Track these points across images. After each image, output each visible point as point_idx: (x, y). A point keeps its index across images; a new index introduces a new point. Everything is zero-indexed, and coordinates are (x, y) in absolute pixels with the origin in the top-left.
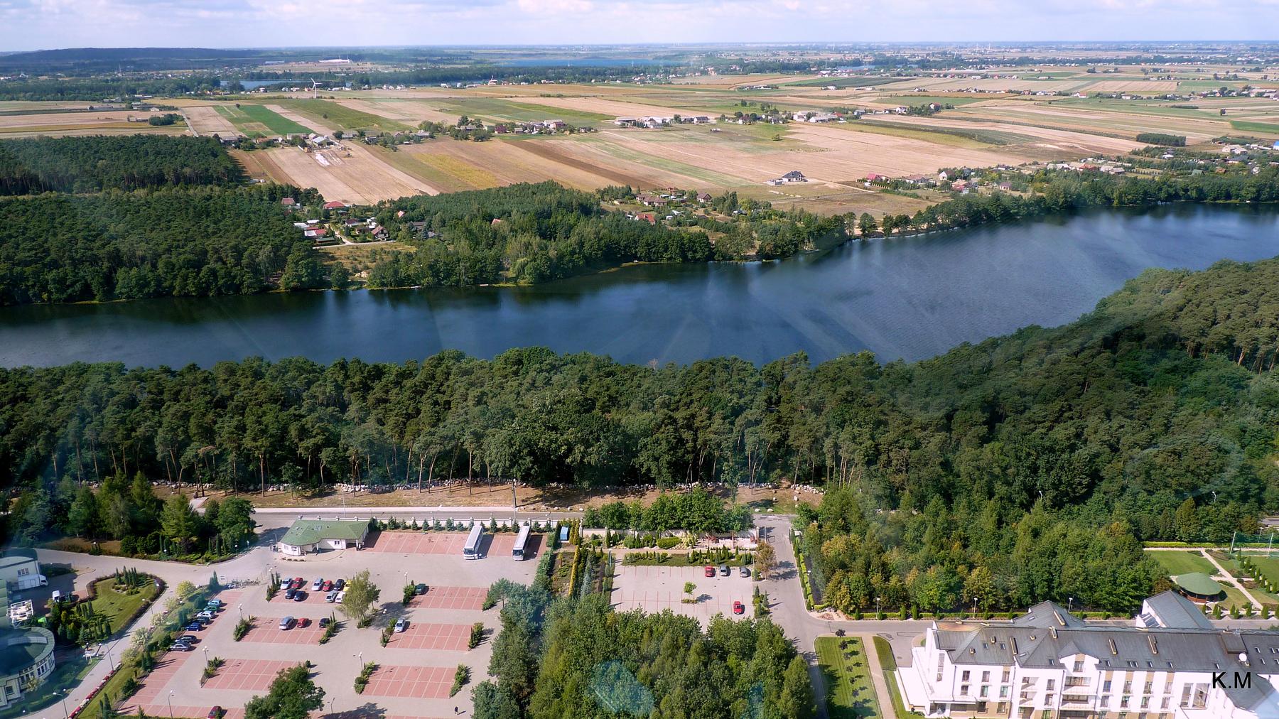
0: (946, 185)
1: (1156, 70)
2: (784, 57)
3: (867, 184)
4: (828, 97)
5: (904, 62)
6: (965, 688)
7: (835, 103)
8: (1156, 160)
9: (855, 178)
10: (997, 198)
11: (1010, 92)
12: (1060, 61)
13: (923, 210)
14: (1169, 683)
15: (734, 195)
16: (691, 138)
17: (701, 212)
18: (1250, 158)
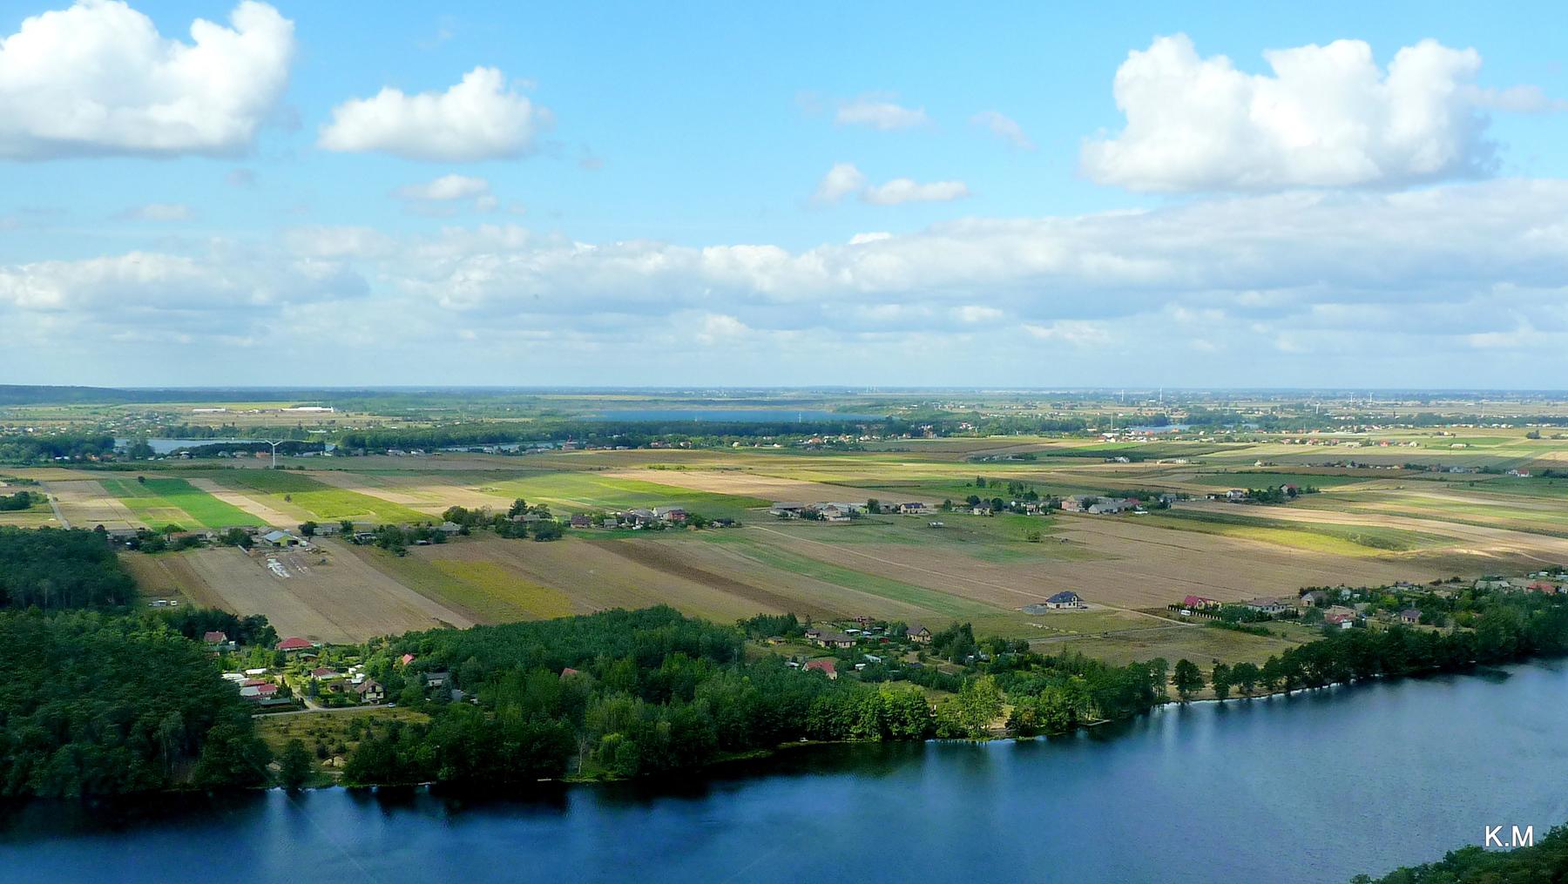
0: (1312, 616)
2: (1044, 412)
3: (1185, 613)
4: (1117, 474)
5: (1235, 420)
7: (1128, 483)
9: (1164, 603)
10: (1397, 633)
11: (1408, 466)
12: (1484, 420)
13: (1279, 656)
15: (967, 630)
16: (895, 537)
17: (912, 657)
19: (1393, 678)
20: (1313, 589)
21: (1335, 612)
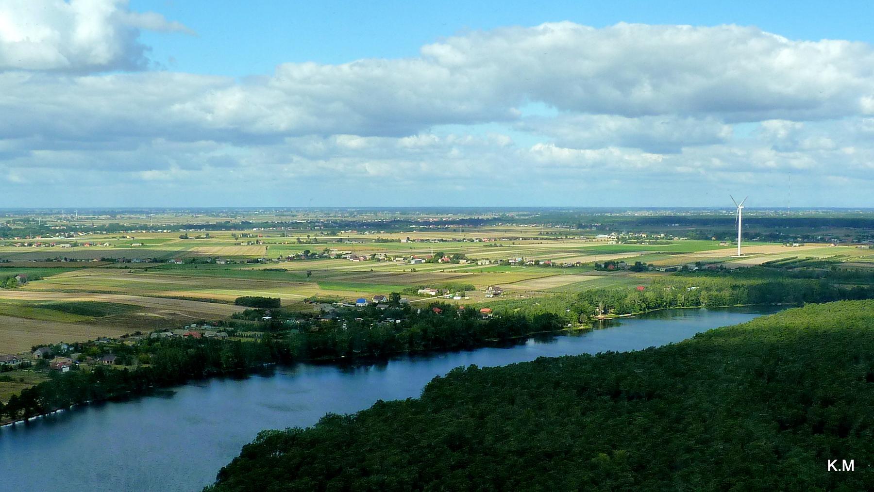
0: (41, 365)
1: (245, 236)
8: (256, 323)
10: (100, 373)
11: (103, 260)
12: (152, 228)
13: (18, 394)
18: (338, 315)
19: (100, 402)
20: (41, 346)
21: (58, 360)
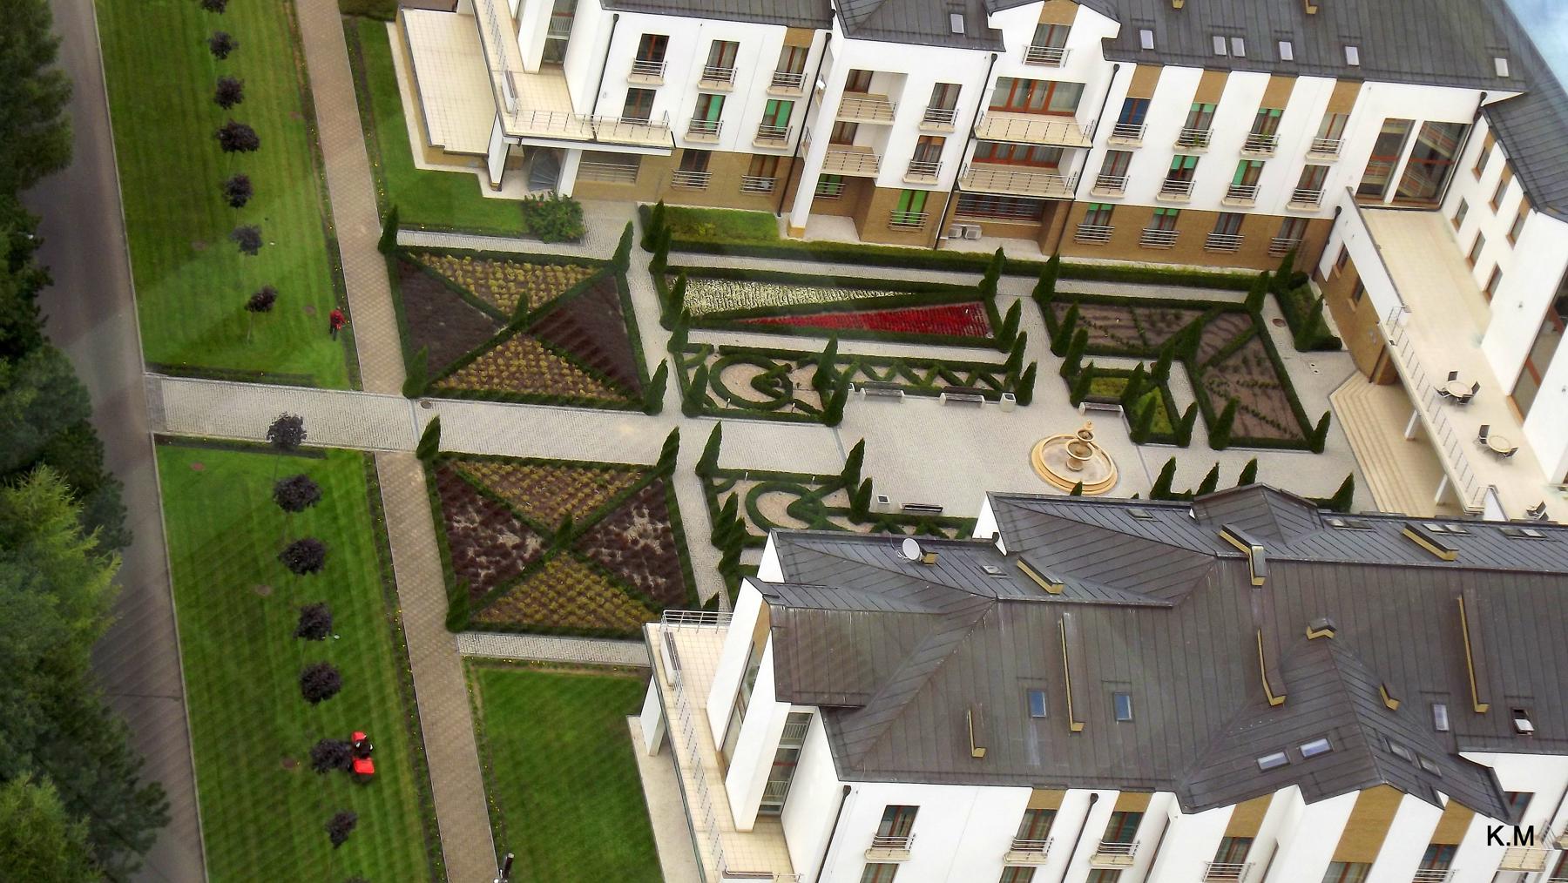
6: (639, 102)
14: (1338, 114)
